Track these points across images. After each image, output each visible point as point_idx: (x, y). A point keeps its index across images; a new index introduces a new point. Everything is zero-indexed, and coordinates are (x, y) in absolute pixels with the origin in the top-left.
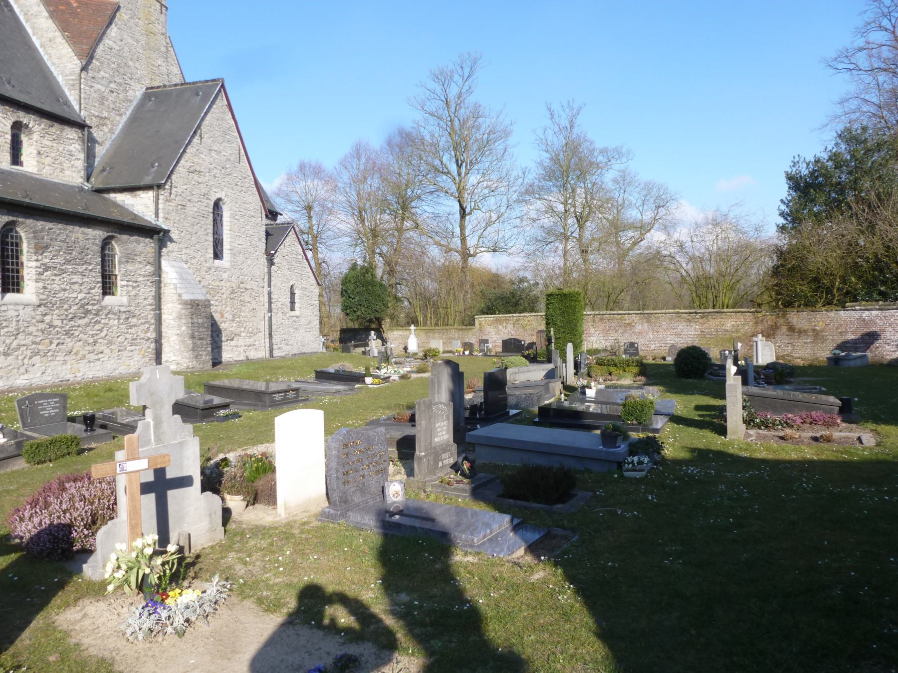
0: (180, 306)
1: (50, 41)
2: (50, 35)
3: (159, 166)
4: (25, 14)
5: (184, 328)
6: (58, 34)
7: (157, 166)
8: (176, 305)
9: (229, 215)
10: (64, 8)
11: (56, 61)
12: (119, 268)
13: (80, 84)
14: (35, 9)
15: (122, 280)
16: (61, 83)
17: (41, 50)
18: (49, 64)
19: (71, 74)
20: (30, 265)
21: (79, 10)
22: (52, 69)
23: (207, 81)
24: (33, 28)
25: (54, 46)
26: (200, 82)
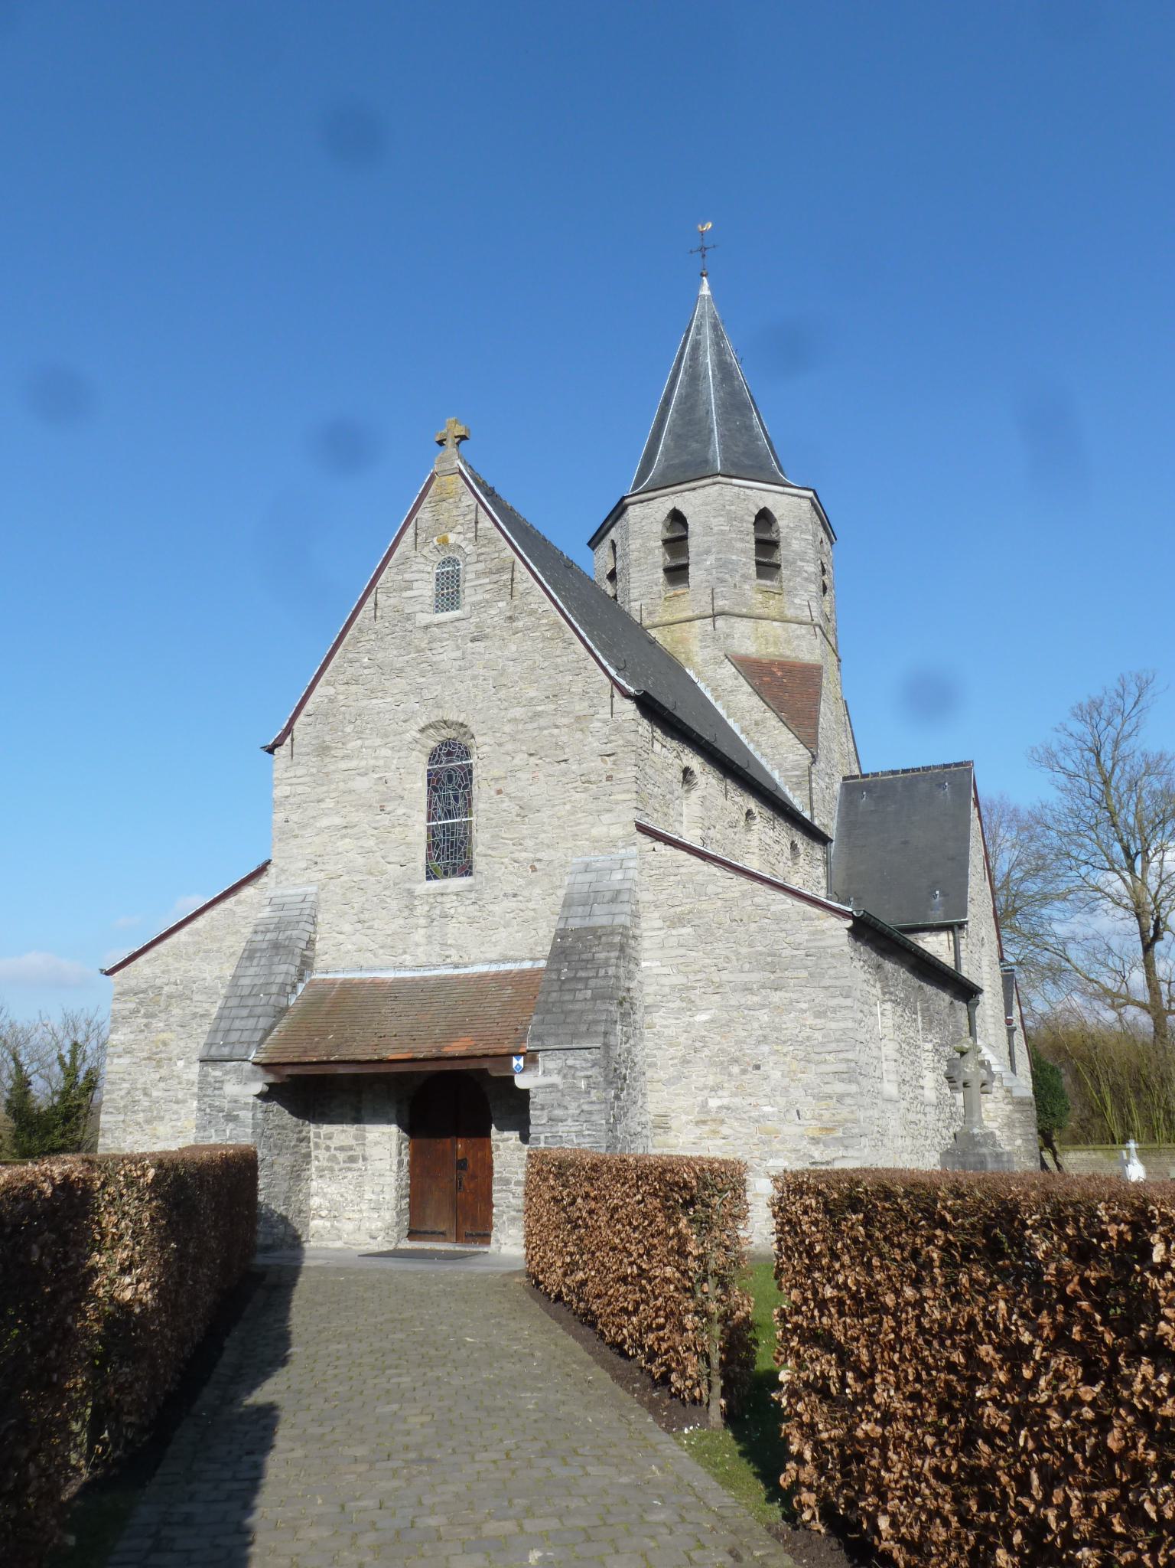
0: (1010, 1107)
1: (757, 724)
2: (757, 716)
3: (944, 894)
4: (714, 690)
5: (1019, 1142)
6: (770, 714)
8: (1002, 1105)
9: (987, 963)
11: (768, 751)
13: (810, 782)
14: (730, 683)
16: (778, 781)
17: (742, 737)
18: (757, 755)
19: (794, 769)
22: (763, 762)
23: (946, 766)
24: (727, 708)
25: (764, 731)
26: (935, 767)
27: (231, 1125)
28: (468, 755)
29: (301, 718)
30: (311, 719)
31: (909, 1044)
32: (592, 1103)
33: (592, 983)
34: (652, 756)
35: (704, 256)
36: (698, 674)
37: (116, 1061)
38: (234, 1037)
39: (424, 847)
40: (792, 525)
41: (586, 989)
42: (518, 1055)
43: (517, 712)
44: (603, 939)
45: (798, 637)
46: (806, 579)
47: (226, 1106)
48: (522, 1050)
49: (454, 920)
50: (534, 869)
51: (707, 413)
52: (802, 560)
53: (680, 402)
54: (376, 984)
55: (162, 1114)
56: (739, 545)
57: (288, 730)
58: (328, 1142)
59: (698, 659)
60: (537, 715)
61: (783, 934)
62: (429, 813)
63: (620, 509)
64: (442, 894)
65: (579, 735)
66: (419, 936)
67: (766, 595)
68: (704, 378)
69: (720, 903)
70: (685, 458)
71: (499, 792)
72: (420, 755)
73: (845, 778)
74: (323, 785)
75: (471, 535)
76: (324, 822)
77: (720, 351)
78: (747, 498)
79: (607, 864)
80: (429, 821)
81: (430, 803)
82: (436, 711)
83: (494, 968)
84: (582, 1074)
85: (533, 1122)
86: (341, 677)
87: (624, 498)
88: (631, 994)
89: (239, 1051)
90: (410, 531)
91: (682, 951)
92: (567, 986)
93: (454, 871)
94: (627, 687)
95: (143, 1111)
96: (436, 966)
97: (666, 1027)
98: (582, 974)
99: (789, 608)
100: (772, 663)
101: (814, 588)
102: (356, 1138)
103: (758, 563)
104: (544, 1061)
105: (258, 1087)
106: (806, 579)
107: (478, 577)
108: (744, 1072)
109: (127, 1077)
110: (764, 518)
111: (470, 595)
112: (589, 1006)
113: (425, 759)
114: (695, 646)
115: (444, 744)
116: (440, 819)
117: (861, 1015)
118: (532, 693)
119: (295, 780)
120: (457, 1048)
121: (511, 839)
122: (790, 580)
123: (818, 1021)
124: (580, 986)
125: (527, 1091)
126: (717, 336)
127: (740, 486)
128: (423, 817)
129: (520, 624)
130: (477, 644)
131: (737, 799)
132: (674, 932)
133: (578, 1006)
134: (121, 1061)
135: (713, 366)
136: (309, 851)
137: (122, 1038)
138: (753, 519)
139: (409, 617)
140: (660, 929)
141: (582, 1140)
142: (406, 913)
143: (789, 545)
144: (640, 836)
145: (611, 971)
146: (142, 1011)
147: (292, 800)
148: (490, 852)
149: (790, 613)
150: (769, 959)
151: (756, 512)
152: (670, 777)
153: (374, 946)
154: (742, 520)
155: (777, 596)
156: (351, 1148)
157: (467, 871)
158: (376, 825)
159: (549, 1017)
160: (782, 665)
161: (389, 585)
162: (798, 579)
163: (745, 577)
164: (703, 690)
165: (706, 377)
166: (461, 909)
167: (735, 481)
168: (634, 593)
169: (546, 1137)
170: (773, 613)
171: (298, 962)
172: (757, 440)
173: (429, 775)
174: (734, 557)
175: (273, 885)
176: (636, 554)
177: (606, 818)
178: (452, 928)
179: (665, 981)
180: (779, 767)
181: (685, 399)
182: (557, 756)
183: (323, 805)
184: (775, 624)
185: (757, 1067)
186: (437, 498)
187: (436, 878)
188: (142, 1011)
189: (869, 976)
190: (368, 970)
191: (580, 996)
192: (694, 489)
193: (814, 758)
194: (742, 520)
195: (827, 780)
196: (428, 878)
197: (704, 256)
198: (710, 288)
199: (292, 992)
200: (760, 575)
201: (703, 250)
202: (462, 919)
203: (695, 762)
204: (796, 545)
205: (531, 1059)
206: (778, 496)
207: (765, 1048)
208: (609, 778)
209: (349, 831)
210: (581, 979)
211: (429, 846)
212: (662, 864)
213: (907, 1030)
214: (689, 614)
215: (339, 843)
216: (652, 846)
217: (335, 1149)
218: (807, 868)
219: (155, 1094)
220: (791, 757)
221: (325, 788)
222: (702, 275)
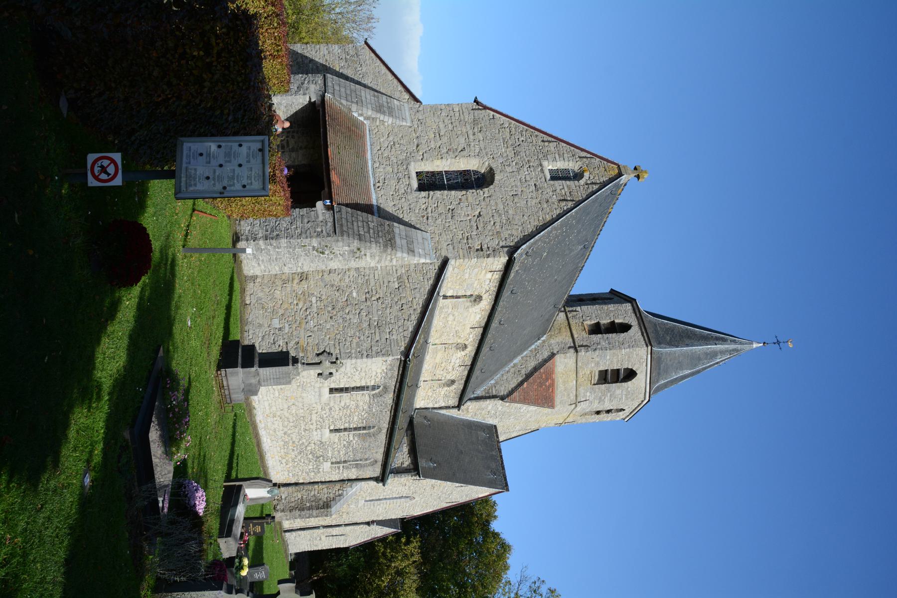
3: (434, 468)
7: (434, 466)
10: (544, 377)
11: (505, 377)
12: (353, 464)
15: (343, 467)
20: (350, 435)
21: (544, 387)
27: (296, 88)
29: (492, 113)
31: (350, 416)
32: (310, 234)
33: (367, 235)
34: (484, 272)
35: (775, 343)
36: (544, 342)
37: (325, 48)
38: (337, 88)
39: (432, 170)
40: (629, 389)
41: (364, 232)
42: (331, 202)
43: (501, 207)
44: (389, 242)
45: (568, 395)
46: (600, 398)
47: (305, 85)
48: (334, 204)
49: (396, 183)
50: (423, 217)
51: (687, 345)
52: (611, 395)
53: (692, 331)
54: (364, 152)
55: (301, 68)
56: (615, 360)
57: (485, 108)
58: (290, 136)
59: (552, 341)
60: (500, 215)
61: (397, 328)
62: (448, 171)
63: (630, 300)
64: (409, 178)
65: (491, 233)
66: (389, 169)
67: (590, 376)
68: (706, 343)
69: (411, 299)
70: (661, 333)
71: (460, 199)
72: (477, 165)
73: (495, 426)
74: (459, 124)
75: (589, 182)
76: (442, 126)
77: (722, 352)
78: (641, 364)
79: (427, 248)
80: (445, 171)
81: (454, 171)
82: (499, 171)
84: (324, 229)
85: (301, 210)
86: (513, 129)
87: (635, 300)
88: (364, 257)
89: (330, 89)
90: (589, 155)
92: (365, 224)
93: (420, 180)
94: (517, 253)
95: (303, 61)
96: (375, 178)
97: (349, 277)
98: (371, 231)
99: (584, 389)
100: (553, 380)
101: (597, 406)
102: (293, 148)
103: (606, 371)
104: (328, 215)
106: (600, 398)
108: (329, 312)
109: (318, 53)
110: (630, 374)
111: (558, 184)
112: (356, 232)
113: (475, 168)
114: (559, 339)
116: (446, 176)
117: (359, 369)
118: (511, 212)
119: (461, 112)
120: (334, 177)
121: (437, 206)
122: (599, 389)
123: (355, 344)
124: (366, 230)
125: (315, 207)
126: (730, 351)
127: (647, 359)
128: (446, 169)
129: (545, 206)
130: (534, 187)
131: (471, 336)
132: (395, 279)
133: (355, 228)
134: (325, 50)
135: (713, 348)
136: (427, 120)
137: (336, 50)
138: (630, 367)
140: (397, 273)
141: (293, 230)
142: (399, 162)
143: (619, 388)
146: (348, 57)
147: (451, 112)
148: (430, 198)
149: (581, 390)
150: (384, 322)
151: (634, 369)
152: (475, 285)
153: (383, 149)
154: (629, 361)
155: (590, 382)
156: (288, 146)
158: (441, 147)
159: (350, 215)
160: (552, 385)
161: (561, 147)
162: (600, 394)
163: (598, 364)
164: (536, 344)
165: (707, 344)
166: (402, 186)
167: (649, 356)
168: (584, 308)
169: (294, 215)
170: (579, 381)
171: (373, 116)
172: (675, 373)
173: (467, 171)
174: (608, 357)
175: (410, 106)
176: (606, 308)
177: (451, 247)
178: (393, 183)
179: (372, 276)
180: (497, 383)
181: (694, 334)
182: (480, 224)
183: (450, 125)
184: (575, 382)
185: (331, 318)
186: (606, 167)
187: (417, 176)
188: (348, 57)
189: (380, 377)
190: (371, 148)
191: (361, 229)
192: (643, 335)
193: (502, 398)
194: (629, 361)
195: (493, 412)
196: (417, 173)
197: (775, 343)
198: (757, 348)
199: (359, 114)
200: (600, 372)
201: (778, 342)
202: (397, 187)
203: (486, 304)
204: (618, 392)
205: (330, 208)
206: (644, 380)
207: (341, 321)
209: (438, 136)
210: (369, 231)
211: (433, 172)
212: (428, 273)
213: (357, 414)
214: (576, 336)
215: (432, 133)
216: (437, 268)
217: (287, 140)
218: (443, 393)
219: (311, 65)
220: (502, 389)
221: (458, 125)
222: (764, 343)
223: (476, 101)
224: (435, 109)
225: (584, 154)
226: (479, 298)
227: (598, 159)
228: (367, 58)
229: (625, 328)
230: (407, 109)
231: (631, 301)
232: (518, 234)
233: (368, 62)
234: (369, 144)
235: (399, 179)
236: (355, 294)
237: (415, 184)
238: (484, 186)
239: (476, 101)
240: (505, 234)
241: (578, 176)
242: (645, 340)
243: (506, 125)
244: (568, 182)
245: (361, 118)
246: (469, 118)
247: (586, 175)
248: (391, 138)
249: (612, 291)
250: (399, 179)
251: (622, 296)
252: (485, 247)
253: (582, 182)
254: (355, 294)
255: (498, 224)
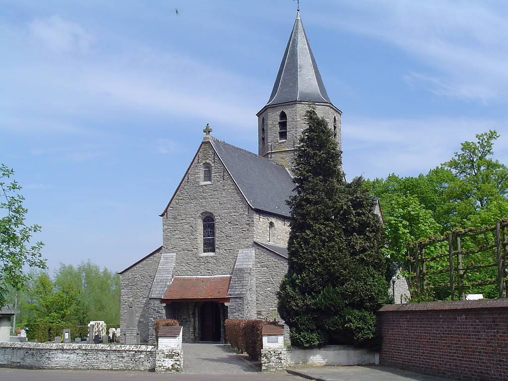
28: (213, 221)
30: (172, 209)
57: (166, 211)
76: (177, 236)
81: (204, 233)
83: (221, 276)
90: (197, 158)
91: (265, 273)
105: (164, 305)
107: (215, 173)
115: (207, 217)
118: (229, 206)
124: (239, 282)
139: (198, 182)
144: (255, 246)
145: (247, 279)
153: (190, 270)
156: (186, 319)
157: (213, 251)
167: (303, 103)
203: (273, 220)
208: (248, 230)
215: (181, 242)
223: (161, 216)
224: (166, 239)
225: (196, 161)
226: (271, 224)
227: (199, 153)
228: (131, 273)
229: (283, 116)
230: (165, 254)
231: (266, 109)
232: (241, 205)
233: (134, 274)
234: (187, 276)
235: (208, 262)
236: (269, 289)
237: (212, 254)
238: (213, 218)
239: (161, 216)
240: (241, 211)
241: (207, 166)
242: (292, 104)
243: (177, 201)
244: (213, 172)
245: (173, 280)
246: (172, 221)
247: (208, 161)
248: (184, 264)
249: (259, 115)
250: (208, 262)
251: (262, 111)
252: (248, 222)
253: (213, 165)
254: (269, 289)
255: (236, 214)
